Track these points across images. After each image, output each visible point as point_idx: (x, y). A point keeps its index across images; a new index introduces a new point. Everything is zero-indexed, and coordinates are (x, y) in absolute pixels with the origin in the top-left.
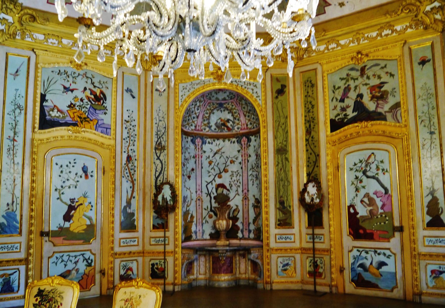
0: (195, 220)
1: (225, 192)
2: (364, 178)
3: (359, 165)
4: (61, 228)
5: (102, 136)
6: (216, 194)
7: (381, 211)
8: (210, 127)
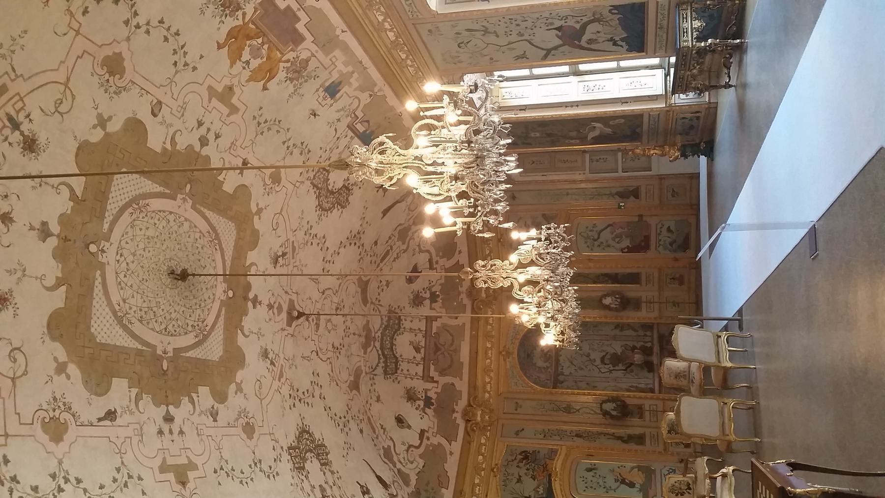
0: (635, 385)
1: (608, 356)
2: (600, 240)
3: (588, 244)
4: (640, 490)
5: (560, 455)
6: (611, 365)
7: (626, 230)
8: (548, 367)
